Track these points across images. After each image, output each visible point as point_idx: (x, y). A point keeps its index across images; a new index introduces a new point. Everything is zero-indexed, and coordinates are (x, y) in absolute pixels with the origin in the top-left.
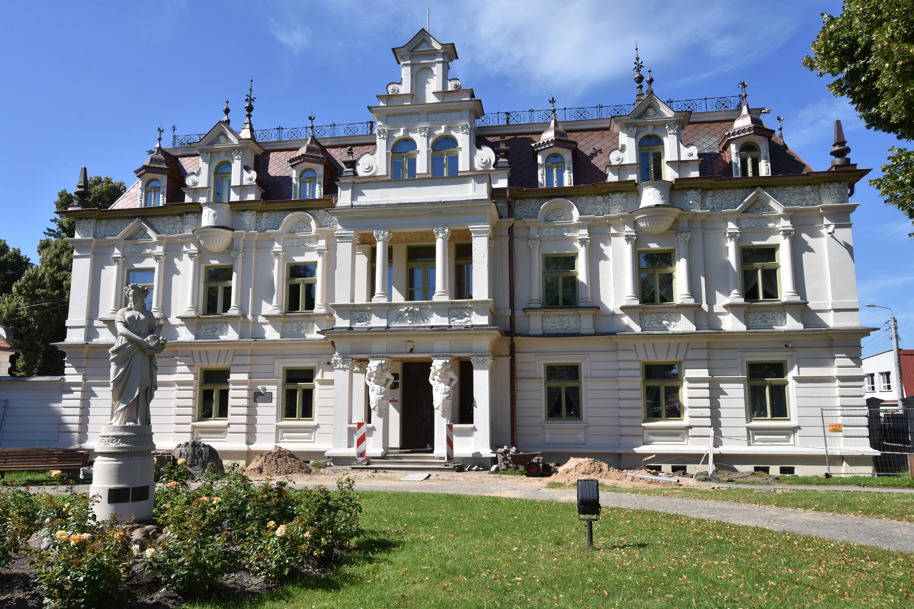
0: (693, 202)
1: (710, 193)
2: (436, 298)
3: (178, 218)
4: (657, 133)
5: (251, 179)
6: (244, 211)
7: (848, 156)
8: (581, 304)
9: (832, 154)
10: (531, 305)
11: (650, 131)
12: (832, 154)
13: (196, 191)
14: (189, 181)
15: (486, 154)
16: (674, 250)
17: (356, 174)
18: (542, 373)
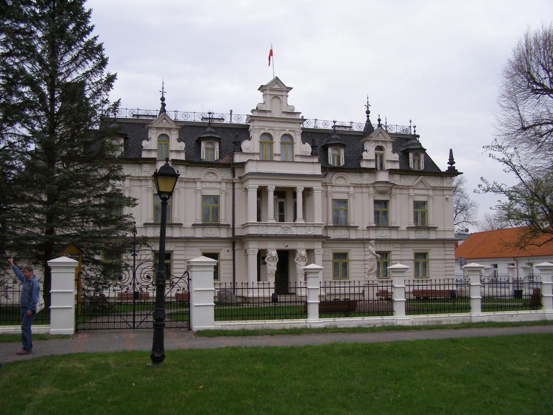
0: (397, 180)
1: (403, 176)
2: (298, 222)
3: (137, 165)
4: (383, 145)
5: (181, 147)
6: (179, 165)
7: (454, 165)
8: (351, 225)
9: (448, 163)
10: (329, 225)
11: (380, 144)
12: (448, 163)
13: (150, 151)
14: (145, 143)
15: (307, 148)
16: (388, 201)
17: (241, 150)
18: (331, 257)
